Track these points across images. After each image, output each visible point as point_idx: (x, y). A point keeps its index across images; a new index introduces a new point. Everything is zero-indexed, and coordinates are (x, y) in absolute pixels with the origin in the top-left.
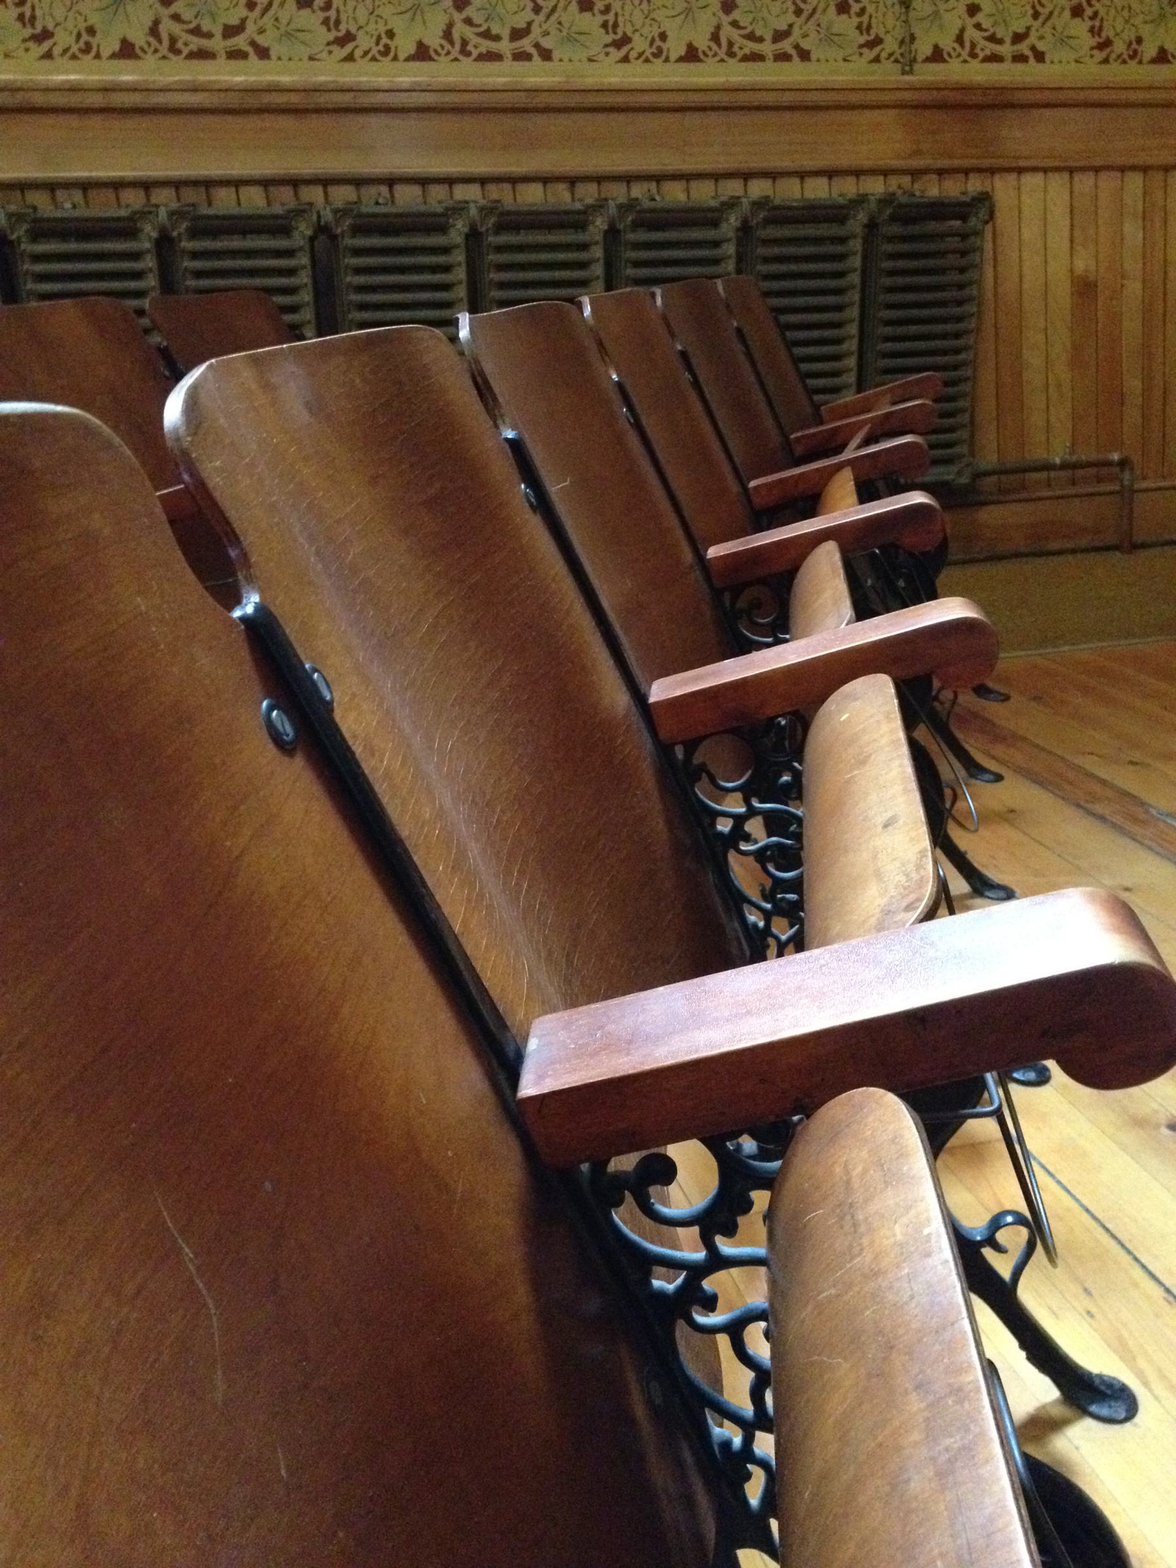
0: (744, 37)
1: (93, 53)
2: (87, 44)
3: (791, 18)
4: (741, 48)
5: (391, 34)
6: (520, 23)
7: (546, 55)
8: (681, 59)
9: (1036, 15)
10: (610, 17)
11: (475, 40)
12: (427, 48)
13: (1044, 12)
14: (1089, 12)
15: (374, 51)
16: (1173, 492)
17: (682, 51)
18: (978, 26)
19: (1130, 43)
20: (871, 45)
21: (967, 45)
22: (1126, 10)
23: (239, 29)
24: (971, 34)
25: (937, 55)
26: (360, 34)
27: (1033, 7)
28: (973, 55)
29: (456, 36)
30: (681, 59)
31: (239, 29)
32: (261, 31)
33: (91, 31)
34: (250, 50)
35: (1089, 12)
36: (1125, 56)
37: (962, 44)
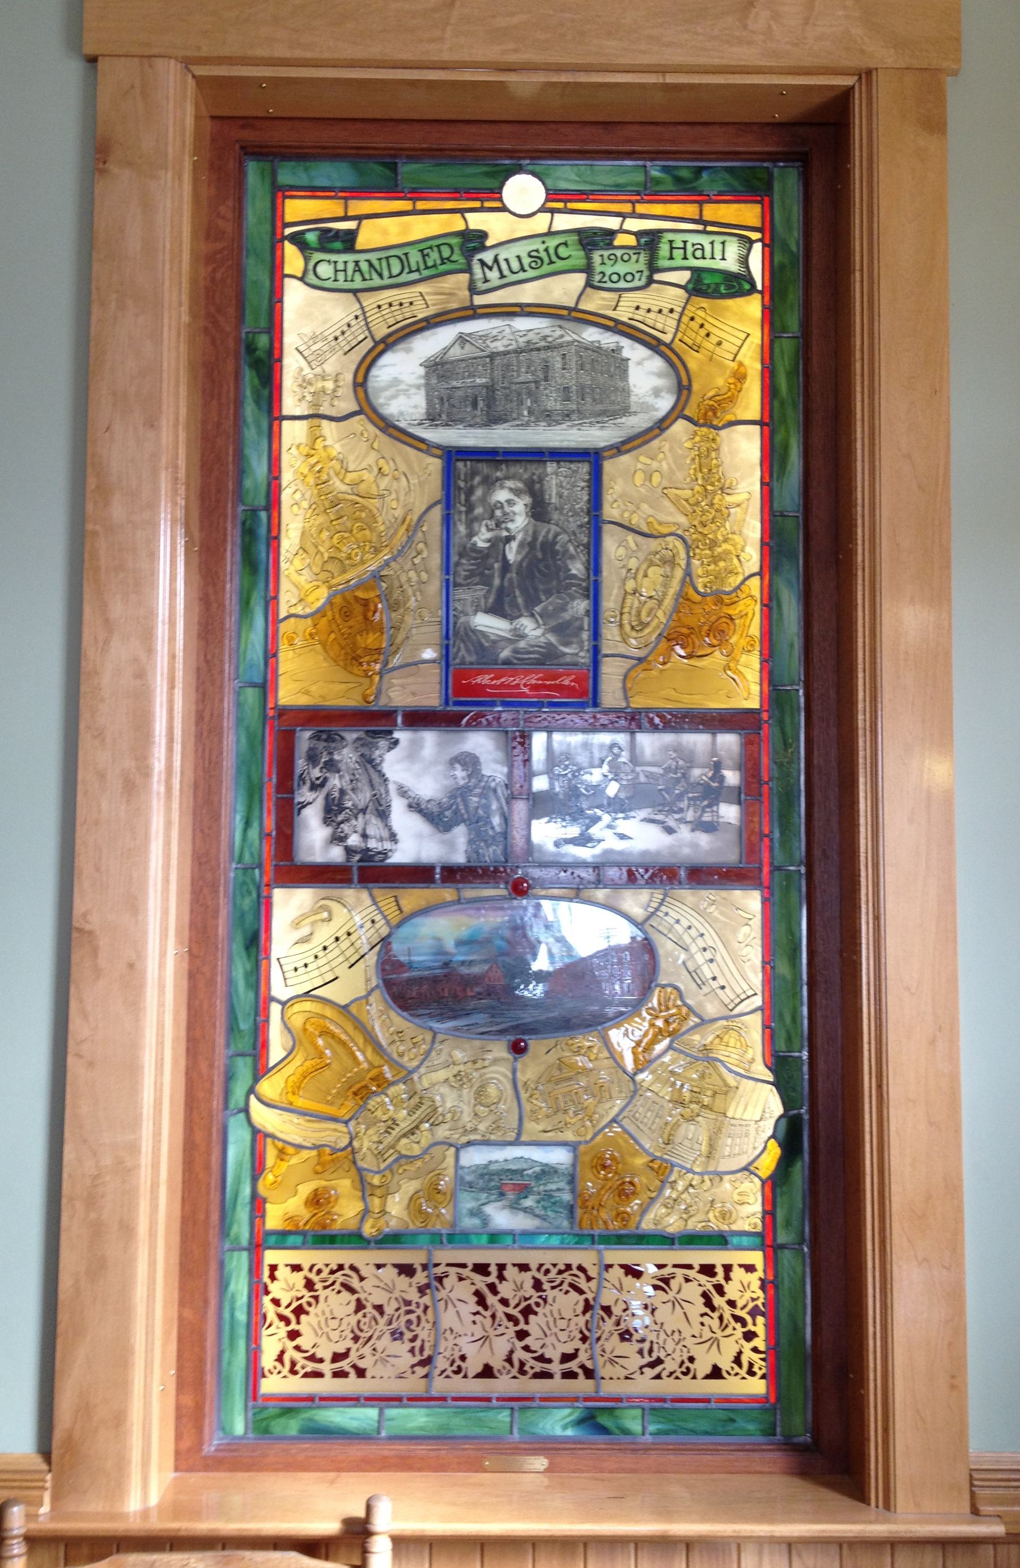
0: (534, 1358)
1: (691, 1375)
2: (459, 1367)
3: (349, 1343)
4: (303, 1368)
5: (463, 1358)
6: (569, 1349)
7: (361, 1373)
8: (478, 1376)
9: (356, 1339)
10: (417, 1344)
11: (533, 1363)
12: (720, 1370)
13: (364, 1335)
14: (408, 1335)
15: (449, 1372)
16: (1014, 1549)
17: (708, 1370)
18: (526, 1348)
19: (683, 1362)
20: (652, 1365)
21: (516, 1364)
22: (676, 1334)
23: (573, 1356)
24: (520, 1355)
25: (716, 1373)
26: (668, 1360)
27: (581, 1332)
28: (522, 1371)
29: (515, 1358)
30: (478, 1376)
31: (573, 1356)
32: (361, 1357)
33: (691, 1359)
34: (580, 1371)
35: (408, 1335)
36: (449, 1372)
37: (740, 1366)
